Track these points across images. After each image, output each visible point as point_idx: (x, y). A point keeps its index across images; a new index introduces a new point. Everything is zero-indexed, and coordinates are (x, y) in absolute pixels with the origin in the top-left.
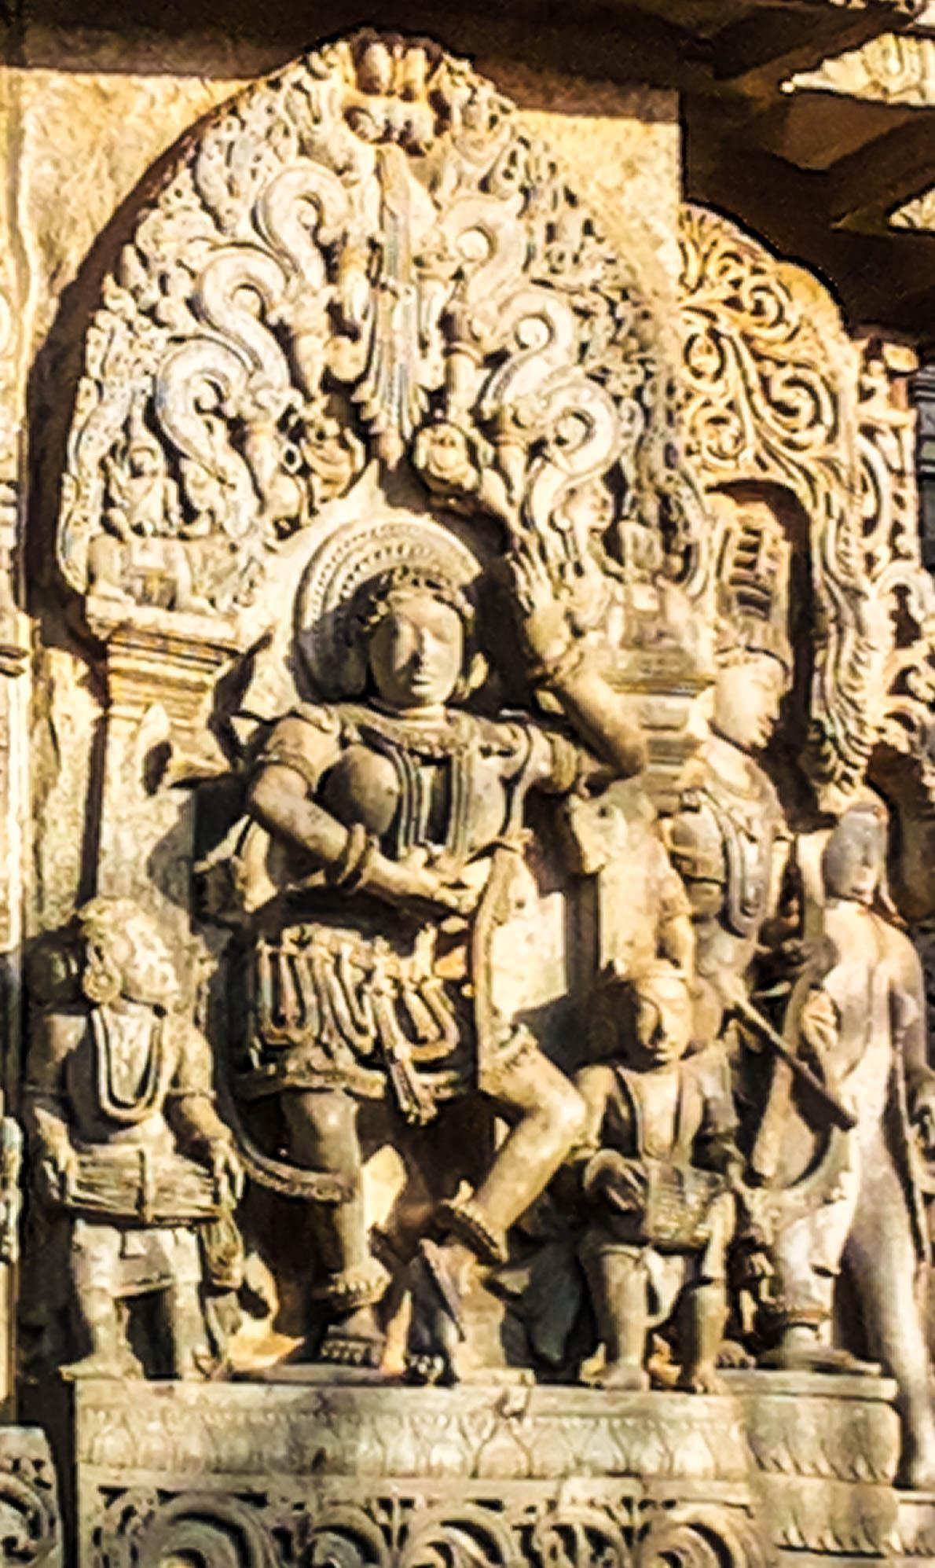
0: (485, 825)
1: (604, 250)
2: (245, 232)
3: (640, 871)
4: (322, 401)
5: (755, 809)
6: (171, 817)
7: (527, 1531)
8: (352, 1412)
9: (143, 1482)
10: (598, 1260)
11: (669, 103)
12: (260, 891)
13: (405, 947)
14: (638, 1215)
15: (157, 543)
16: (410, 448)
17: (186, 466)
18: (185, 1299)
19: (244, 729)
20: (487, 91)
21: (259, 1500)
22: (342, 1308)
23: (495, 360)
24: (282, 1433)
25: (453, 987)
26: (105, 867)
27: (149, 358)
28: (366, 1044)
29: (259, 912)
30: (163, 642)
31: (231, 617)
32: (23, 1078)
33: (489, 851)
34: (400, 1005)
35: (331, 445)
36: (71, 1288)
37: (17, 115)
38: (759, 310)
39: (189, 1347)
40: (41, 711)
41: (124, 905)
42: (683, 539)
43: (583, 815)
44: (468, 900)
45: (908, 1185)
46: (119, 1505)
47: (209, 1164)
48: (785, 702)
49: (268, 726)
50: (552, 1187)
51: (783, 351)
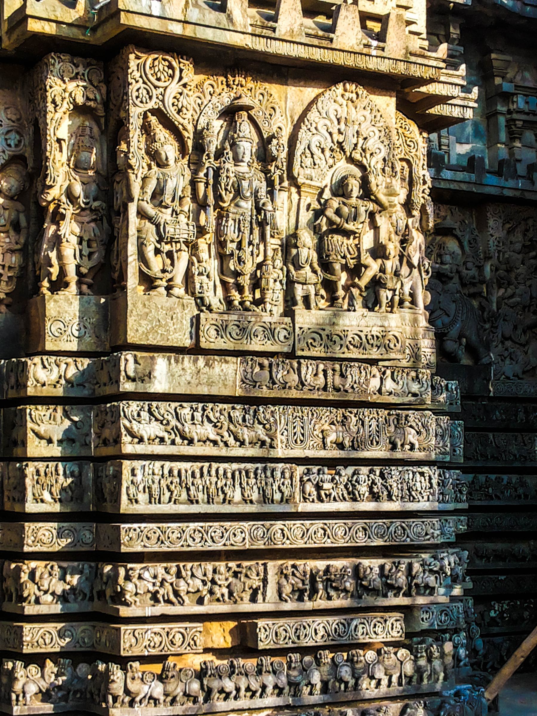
0: (362, 219)
1: (384, 120)
2: (325, 116)
3: (386, 226)
4: (337, 145)
5: (402, 214)
6: (311, 216)
7: (366, 336)
8: (339, 315)
9: (306, 326)
10: (378, 291)
11: (395, 94)
12: (324, 228)
13: (348, 238)
14: (385, 284)
15: (309, 169)
16: (351, 153)
17: (314, 156)
18: (313, 297)
19: (322, 201)
20: (365, 92)
21: (324, 330)
22: (337, 298)
23: (365, 139)
24: (328, 319)
25: (356, 245)
26: (300, 224)
27: (308, 138)
28: (342, 255)
29: (324, 232)
30: (310, 186)
31: (321, 182)
32: (286, 258)
33: (363, 223)
34: (348, 248)
35: (338, 153)
36: (294, 294)
37: (287, 94)
38: (405, 128)
39: (313, 305)
40: (289, 197)
41: (304, 231)
42: (395, 170)
43: (377, 216)
44: (360, 231)
45: (421, 277)
46: (302, 330)
47: (317, 274)
48: (407, 196)
49: (326, 201)
50: (371, 279)
51: (409, 136)
